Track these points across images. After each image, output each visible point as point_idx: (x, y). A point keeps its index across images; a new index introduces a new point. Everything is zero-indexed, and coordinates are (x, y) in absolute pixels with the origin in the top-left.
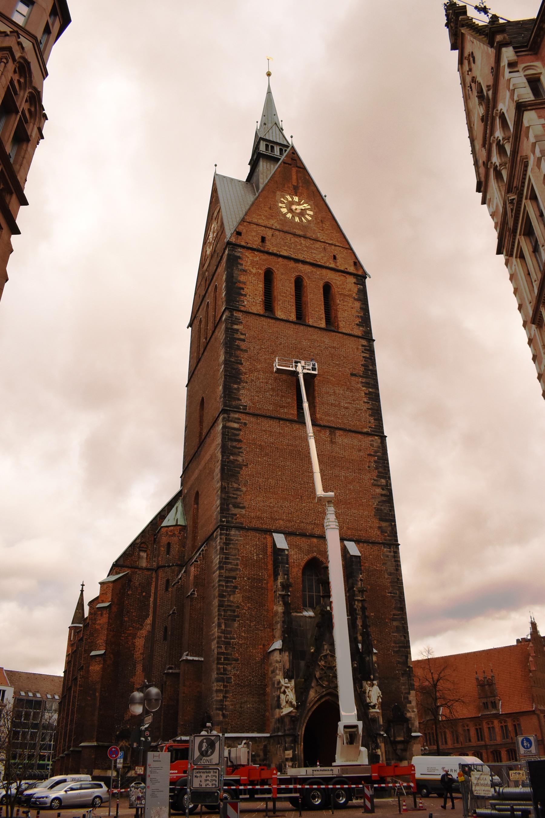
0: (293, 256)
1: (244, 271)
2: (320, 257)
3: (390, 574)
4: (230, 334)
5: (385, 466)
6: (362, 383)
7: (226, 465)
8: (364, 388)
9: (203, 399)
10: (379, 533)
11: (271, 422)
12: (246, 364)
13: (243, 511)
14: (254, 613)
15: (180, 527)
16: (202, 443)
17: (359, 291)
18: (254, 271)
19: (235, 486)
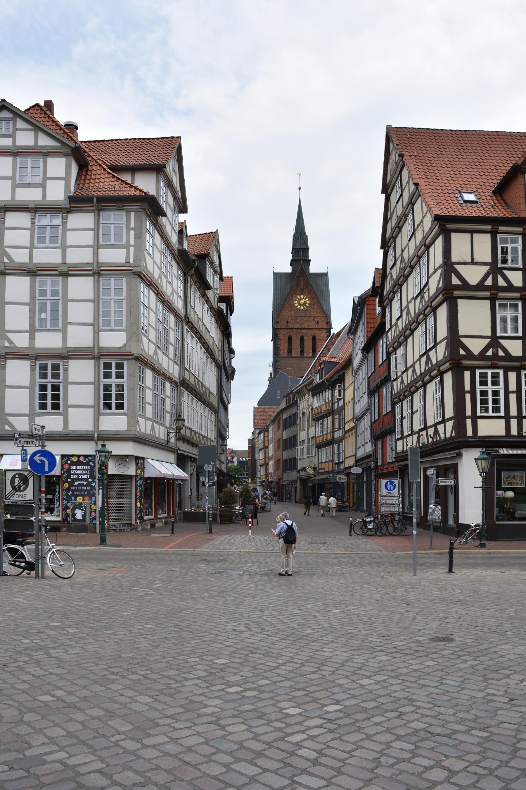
2: (311, 325)
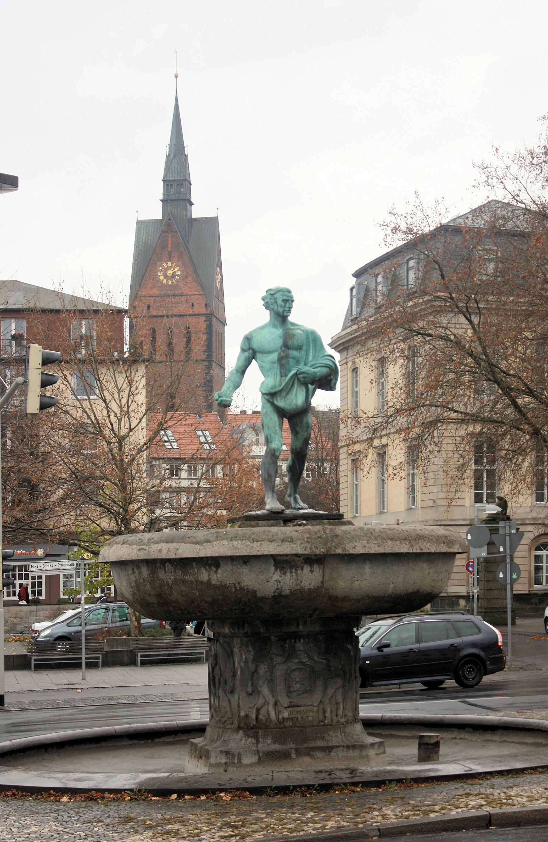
2: (183, 308)
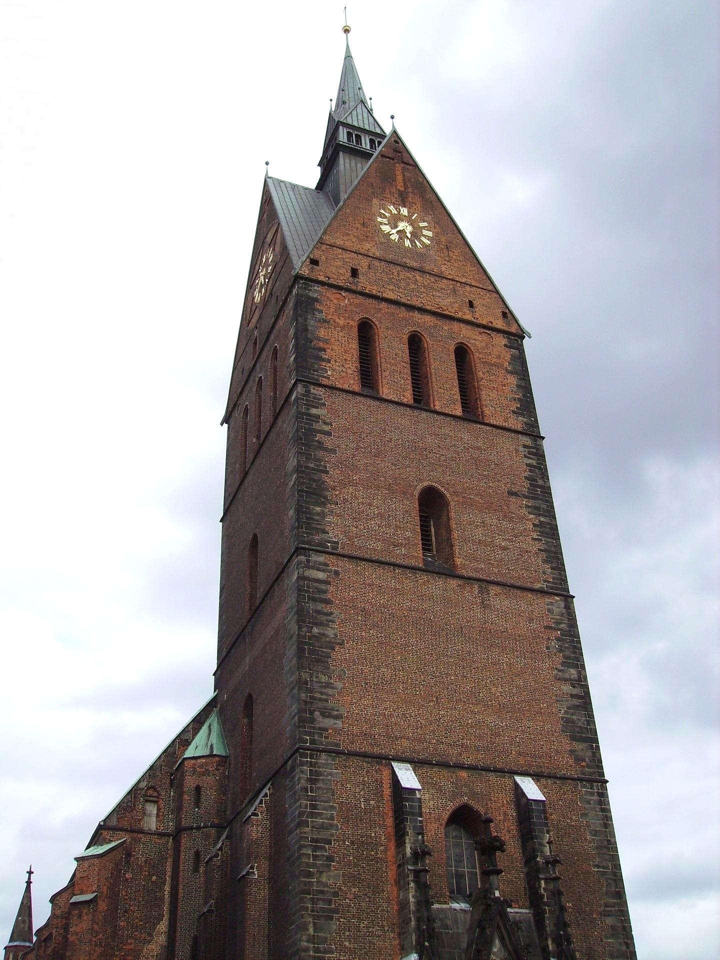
0: (403, 300)
1: (325, 321)
2: (447, 303)
3: (595, 833)
4: (306, 423)
5: (575, 647)
6: (527, 507)
7: (306, 644)
8: (531, 516)
9: (255, 537)
10: (571, 762)
11: (380, 570)
12: (335, 473)
13: (339, 724)
14: (364, 904)
15: (217, 759)
16: (256, 611)
17: (513, 358)
18: (341, 322)
19: (324, 679)
